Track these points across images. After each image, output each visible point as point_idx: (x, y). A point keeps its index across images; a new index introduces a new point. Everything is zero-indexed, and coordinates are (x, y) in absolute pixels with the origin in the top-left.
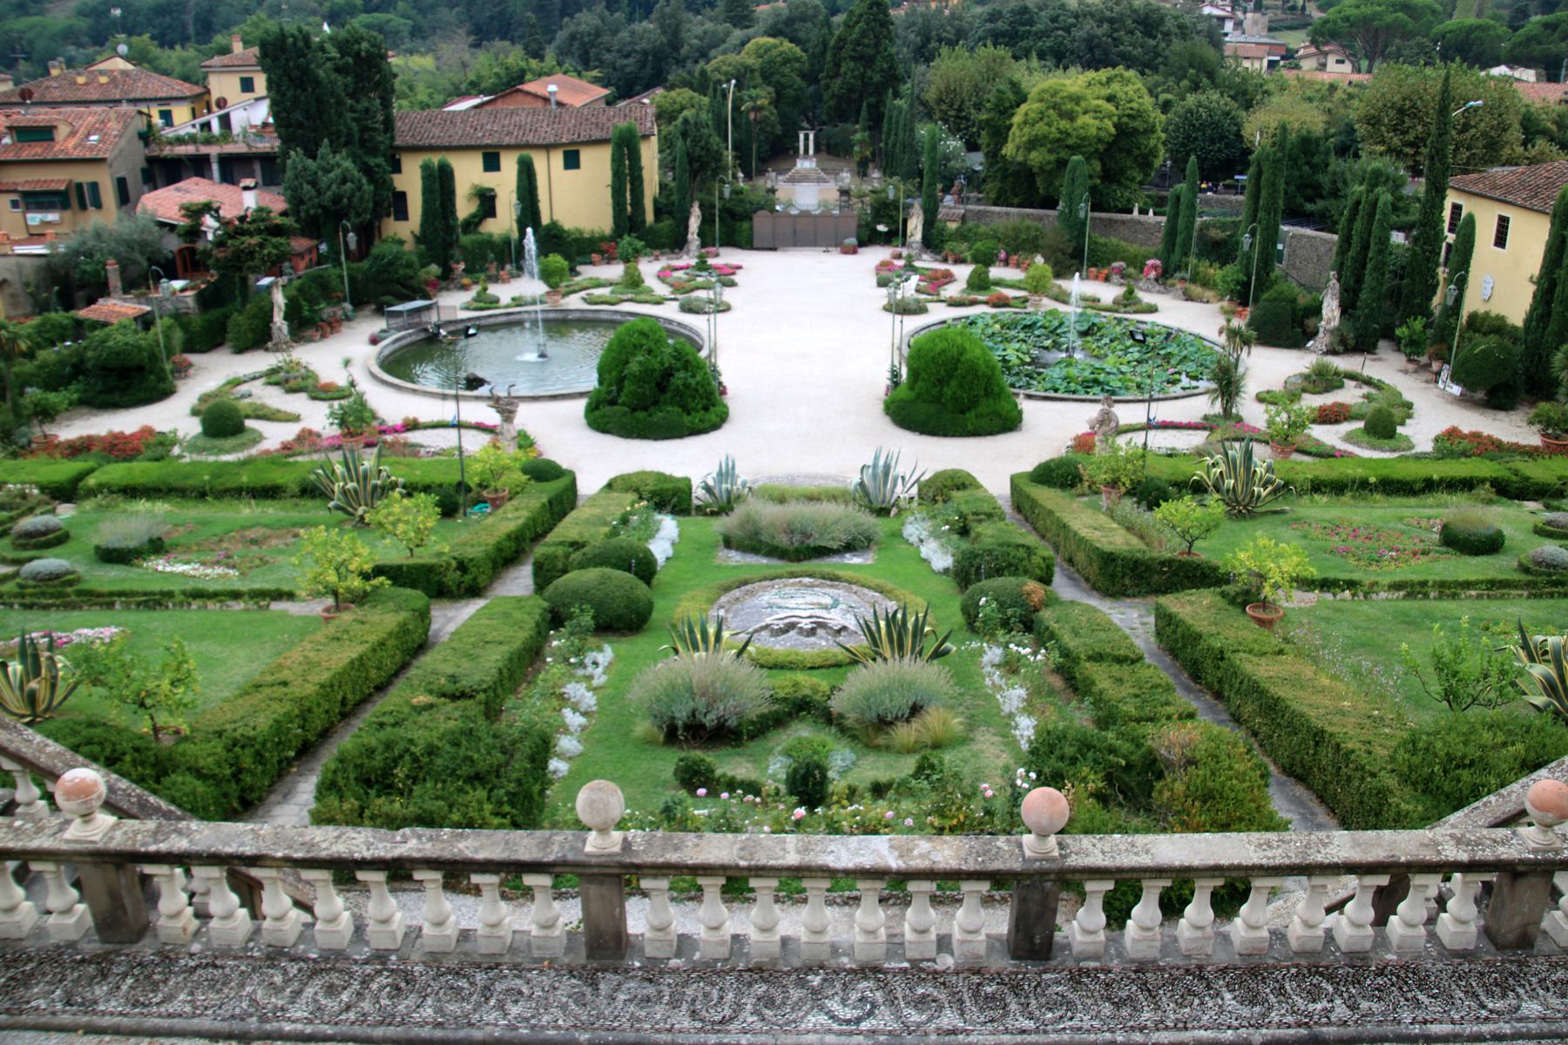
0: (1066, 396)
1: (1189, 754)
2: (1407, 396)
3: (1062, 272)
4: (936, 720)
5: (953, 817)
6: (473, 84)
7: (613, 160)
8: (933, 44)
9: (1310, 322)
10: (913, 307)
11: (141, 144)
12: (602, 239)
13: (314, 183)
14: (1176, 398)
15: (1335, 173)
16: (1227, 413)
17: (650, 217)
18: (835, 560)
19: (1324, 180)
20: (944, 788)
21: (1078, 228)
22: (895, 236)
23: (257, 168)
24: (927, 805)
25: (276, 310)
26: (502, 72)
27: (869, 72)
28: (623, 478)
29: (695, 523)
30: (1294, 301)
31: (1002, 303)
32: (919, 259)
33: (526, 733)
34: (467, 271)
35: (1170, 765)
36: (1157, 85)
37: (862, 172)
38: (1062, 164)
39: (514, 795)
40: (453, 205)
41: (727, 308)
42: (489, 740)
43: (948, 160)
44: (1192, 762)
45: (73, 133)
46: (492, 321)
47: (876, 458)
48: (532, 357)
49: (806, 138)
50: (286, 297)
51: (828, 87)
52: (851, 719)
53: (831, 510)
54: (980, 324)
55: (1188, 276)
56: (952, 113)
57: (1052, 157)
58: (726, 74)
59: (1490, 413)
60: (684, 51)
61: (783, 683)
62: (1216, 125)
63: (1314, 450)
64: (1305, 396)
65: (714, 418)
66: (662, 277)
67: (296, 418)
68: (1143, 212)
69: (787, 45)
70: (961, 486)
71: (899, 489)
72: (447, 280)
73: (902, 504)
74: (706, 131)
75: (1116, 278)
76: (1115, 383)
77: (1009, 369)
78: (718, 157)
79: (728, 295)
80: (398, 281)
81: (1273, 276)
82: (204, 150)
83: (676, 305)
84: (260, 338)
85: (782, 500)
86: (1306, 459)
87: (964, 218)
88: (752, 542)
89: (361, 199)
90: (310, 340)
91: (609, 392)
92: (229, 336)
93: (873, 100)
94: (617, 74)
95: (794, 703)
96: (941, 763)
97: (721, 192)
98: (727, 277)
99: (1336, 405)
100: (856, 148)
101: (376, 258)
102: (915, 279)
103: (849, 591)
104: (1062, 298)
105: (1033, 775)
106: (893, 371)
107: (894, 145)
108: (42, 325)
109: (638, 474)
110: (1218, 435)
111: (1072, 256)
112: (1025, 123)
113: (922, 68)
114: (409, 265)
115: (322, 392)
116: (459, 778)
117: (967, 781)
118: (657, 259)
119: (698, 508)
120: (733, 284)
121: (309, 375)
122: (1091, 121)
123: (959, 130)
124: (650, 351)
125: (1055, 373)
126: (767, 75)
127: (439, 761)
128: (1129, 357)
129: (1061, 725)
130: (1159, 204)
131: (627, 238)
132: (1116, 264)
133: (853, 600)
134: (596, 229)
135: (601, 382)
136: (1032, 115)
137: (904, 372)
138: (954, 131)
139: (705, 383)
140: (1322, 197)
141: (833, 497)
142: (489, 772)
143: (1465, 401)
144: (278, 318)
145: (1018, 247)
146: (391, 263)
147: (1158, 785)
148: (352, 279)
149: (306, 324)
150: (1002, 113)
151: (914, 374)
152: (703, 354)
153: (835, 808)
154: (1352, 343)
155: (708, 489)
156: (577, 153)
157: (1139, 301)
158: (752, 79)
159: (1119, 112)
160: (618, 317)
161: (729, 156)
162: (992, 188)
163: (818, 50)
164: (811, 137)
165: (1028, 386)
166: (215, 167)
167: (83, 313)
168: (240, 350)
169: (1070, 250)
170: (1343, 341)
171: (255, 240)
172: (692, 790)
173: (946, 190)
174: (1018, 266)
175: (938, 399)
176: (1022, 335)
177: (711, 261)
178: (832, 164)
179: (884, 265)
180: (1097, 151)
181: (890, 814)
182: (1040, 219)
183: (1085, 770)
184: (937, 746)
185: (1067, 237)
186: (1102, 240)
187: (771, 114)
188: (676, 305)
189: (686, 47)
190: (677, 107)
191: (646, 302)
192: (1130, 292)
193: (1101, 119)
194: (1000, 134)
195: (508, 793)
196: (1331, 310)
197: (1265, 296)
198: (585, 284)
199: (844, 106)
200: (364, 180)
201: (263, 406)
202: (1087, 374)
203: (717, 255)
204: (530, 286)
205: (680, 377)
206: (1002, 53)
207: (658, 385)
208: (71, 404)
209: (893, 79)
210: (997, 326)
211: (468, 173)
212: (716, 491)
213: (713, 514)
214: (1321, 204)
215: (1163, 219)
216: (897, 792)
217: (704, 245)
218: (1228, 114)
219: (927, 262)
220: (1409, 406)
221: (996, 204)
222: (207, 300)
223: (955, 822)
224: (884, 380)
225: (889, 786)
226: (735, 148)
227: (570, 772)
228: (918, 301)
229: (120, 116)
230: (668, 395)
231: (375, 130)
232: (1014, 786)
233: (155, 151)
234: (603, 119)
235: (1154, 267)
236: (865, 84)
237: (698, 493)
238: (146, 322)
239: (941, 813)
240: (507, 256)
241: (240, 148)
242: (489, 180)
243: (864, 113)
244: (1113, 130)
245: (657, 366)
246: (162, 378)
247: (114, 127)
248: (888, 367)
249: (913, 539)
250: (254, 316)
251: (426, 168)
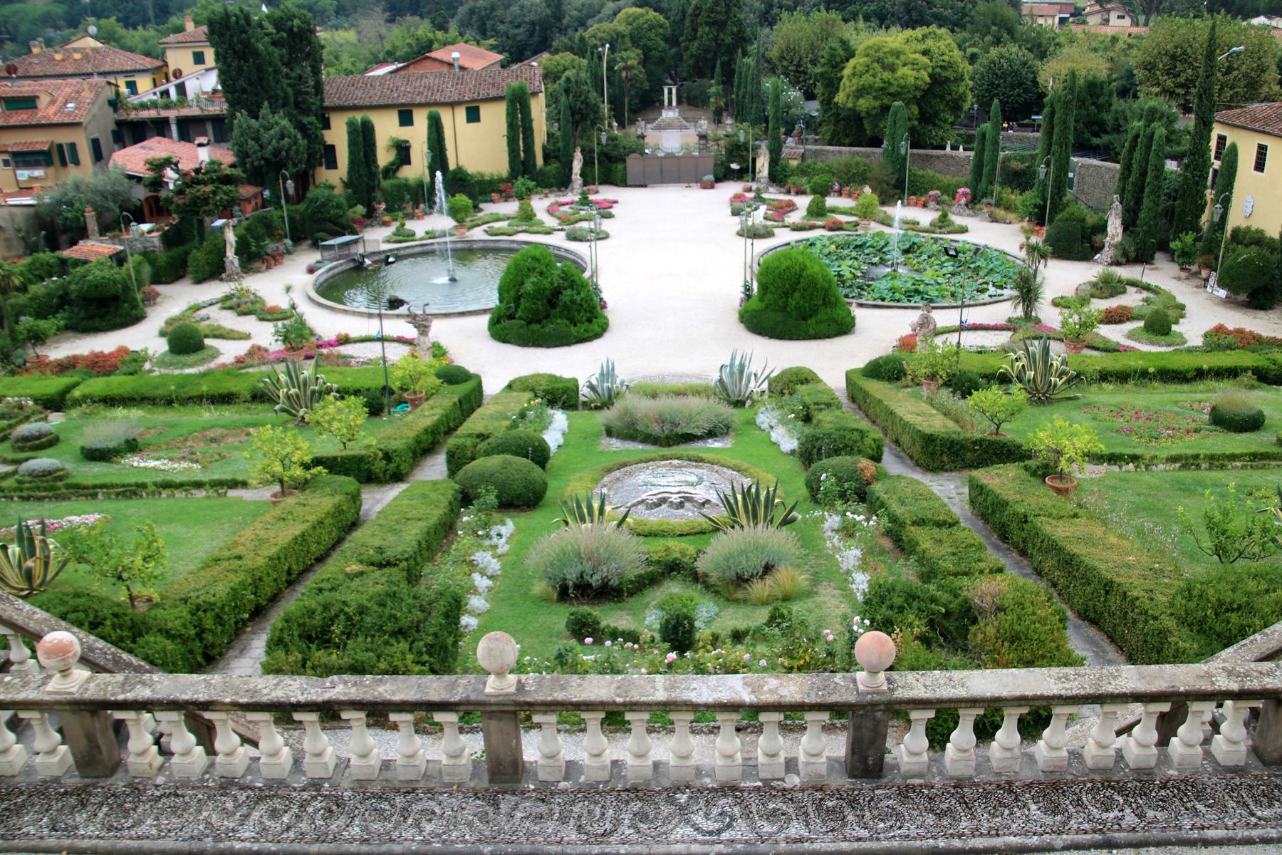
0: (892, 304)
1: (999, 602)
4: (785, 577)
5: (800, 658)
6: (389, 53)
7: (508, 114)
8: (776, 10)
9: (1097, 238)
10: (762, 231)
11: (111, 110)
12: (501, 180)
13: (257, 139)
14: (985, 304)
15: (1117, 112)
16: (1028, 316)
17: (540, 161)
18: (700, 444)
19: (1108, 117)
20: (793, 634)
22: (746, 172)
23: (209, 127)
24: (778, 649)
25: (228, 246)
26: (414, 43)
27: (722, 35)
28: (520, 380)
29: (582, 416)
30: (1083, 220)
31: (837, 227)
32: (767, 192)
33: (441, 594)
34: (388, 210)
35: (982, 611)
36: (965, 41)
37: (717, 119)
38: (885, 109)
39: (432, 646)
40: (375, 155)
41: (606, 236)
42: (411, 601)
43: (790, 108)
44: (1001, 609)
45: (53, 102)
46: (409, 251)
47: (733, 359)
48: (444, 280)
49: (670, 92)
50: (236, 235)
51: (687, 48)
52: (714, 577)
53: (695, 403)
54: (819, 245)
55: (993, 202)
56: (792, 68)
57: (877, 104)
58: (601, 39)
59: (1252, 313)
60: (565, 21)
61: (657, 548)
62: (1016, 73)
63: (1101, 346)
64: (1093, 300)
65: (597, 329)
66: (551, 211)
67: (247, 337)
68: (954, 148)
69: (652, 14)
70: (805, 381)
71: (752, 384)
72: (371, 217)
73: (755, 396)
74: (585, 88)
75: (932, 204)
76: (933, 292)
77: (843, 282)
78: (596, 109)
79: (606, 225)
81: (1065, 199)
82: (164, 114)
83: (563, 234)
84: (215, 271)
85: (654, 395)
87: (803, 157)
88: (629, 431)
89: (297, 152)
90: (258, 271)
91: (509, 308)
92: (190, 269)
93: (725, 59)
94: (510, 42)
95: (666, 565)
96: (789, 612)
97: (599, 139)
98: (605, 211)
99: (1120, 307)
100: (712, 100)
101: (311, 201)
102: (763, 208)
103: (712, 470)
104: (887, 222)
105: (867, 622)
106: (746, 286)
107: (744, 97)
108: (32, 264)
109: (533, 376)
110: (1020, 335)
111: (896, 187)
112: (854, 74)
113: (767, 30)
114: (339, 206)
115: (267, 314)
116: (385, 632)
117: (812, 628)
118: (546, 196)
119: (584, 403)
120: (610, 216)
121: (257, 300)
122: (910, 72)
123: (798, 82)
124: (541, 274)
125: (882, 285)
126: (635, 40)
127: (368, 619)
128: (944, 270)
129: (891, 579)
130: (968, 141)
131: (521, 180)
132: (932, 193)
133: (715, 478)
134: (495, 172)
135: (501, 301)
136: (859, 68)
137: (755, 286)
138: (794, 83)
139: (588, 299)
140: (1106, 132)
141: (697, 392)
142: (410, 628)
143: (1230, 302)
144: (230, 253)
145: (850, 179)
146: (323, 205)
147: (973, 629)
148: (292, 219)
150: (834, 67)
151: (764, 288)
152: (587, 275)
153: (701, 652)
154: (1132, 255)
155: (592, 387)
156: (477, 109)
157: (952, 223)
158: (624, 43)
159: (934, 64)
160: (515, 246)
161: (605, 108)
162: (827, 130)
163: (678, 18)
164: (674, 91)
165: (860, 296)
166: (174, 128)
167: (66, 253)
168: (199, 281)
169: (893, 182)
170: (1125, 254)
171: (210, 188)
172: (581, 641)
173: (788, 133)
174: (850, 196)
175: (784, 309)
176: (854, 254)
177: (592, 197)
178: (692, 113)
179: (737, 197)
180: (915, 97)
181: (747, 656)
182: (868, 156)
183: (912, 617)
184: (786, 598)
185: (891, 170)
186: (920, 173)
187: (640, 72)
188: (563, 234)
189: (568, 18)
190: (561, 68)
191: (538, 233)
192: (945, 216)
193: (918, 70)
194: (833, 85)
195: (426, 645)
196: (1115, 227)
197: (1059, 217)
198: (487, 219)
199: (701, 64)
200: (299, 136)
201: (219, 327)
202: (909, 285)
203: (597, 192)
204: (440, 222)
205: (566, 295)
206: (834, 16)
207: (549, 301)
208: (58, 329)
209: (741, 41)
210: (833, 247)
211: (386, 128)
212: (599, 390)
213: (597, 408)
214: (1105, 139)
215: (972, 154)
216: (753, 638)
217: (585, 184)
218: (1025, 64)
219: (773, 194)
220: (1182, 307)
221: (830, 144)
222: (170, 240)
223: (802, 662)
224: (738, 293)
225: (746, 633)
226: (610, 102)
227: (479, 626)
228: (766, 227)
229: (92, 87)
230: (558, 310)
231: (307, 93)
232: (851, 631)
233: (123, 116)
234: (498, 80)
235: (965, 194)
236: (719, 46)
237: (584, 390)
238: (119, 259)
239: (790, 654)
240: (421, 197)
241: (195, 111)
242: (404, 133)
243: (718, 70)
244: (928, 80)
245: (547, 286)
246: (135, 307)
247: (87, 95)
248: (742, 282)
249: (765, 426)
250: (210, 252)
251: (351, 125)
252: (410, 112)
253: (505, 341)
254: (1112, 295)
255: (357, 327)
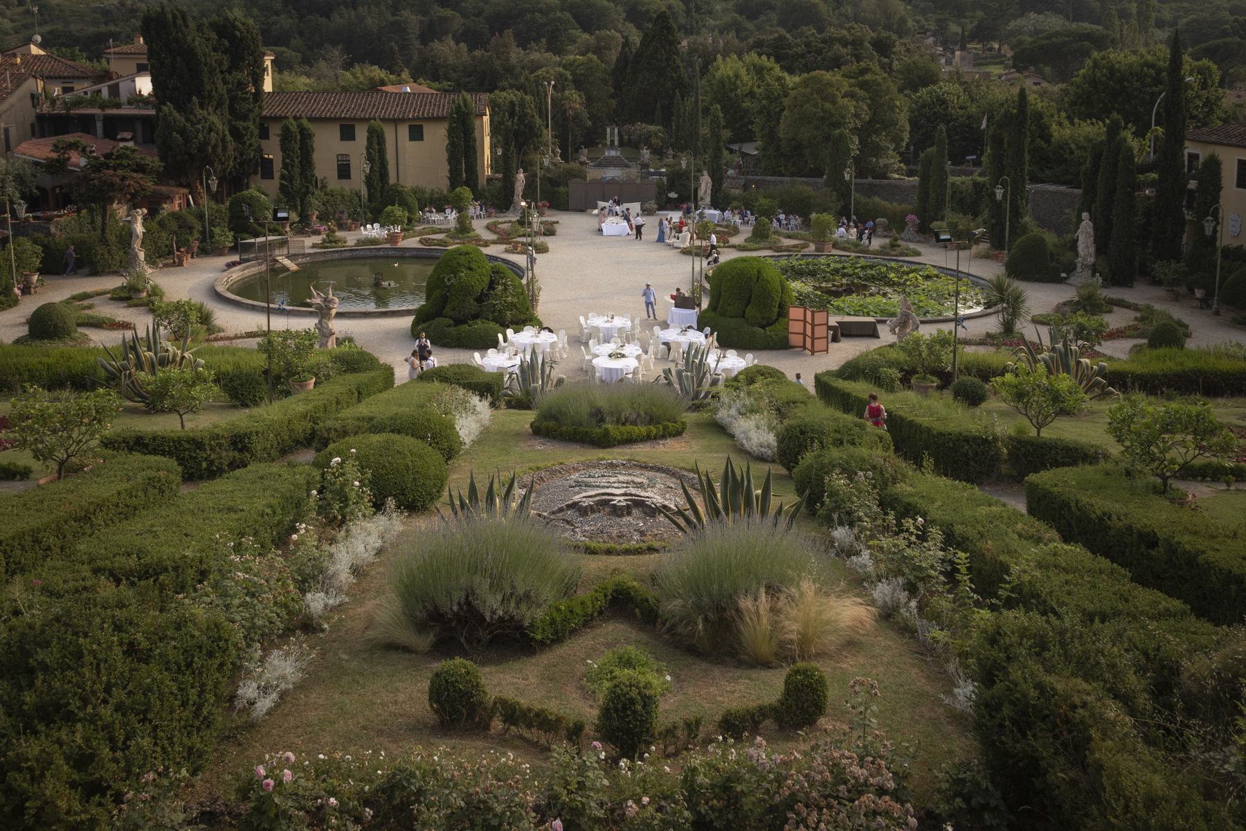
11: (30, 103)
23: (139, 127)
49: (612, 133)
97: (542, 164)
161: (548, 134)
166: (99, 125)
252: (353, 127)
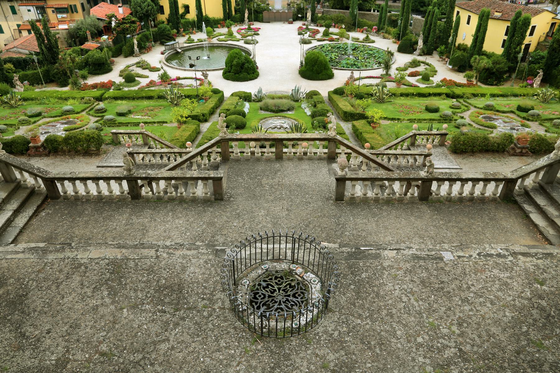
0: (346, 69)
2: (437, 69)
3: (349, 29)
9: (415, 46)
10: (308, 42)
16: (387, 74)
21: (354, 17)
22: (303, 18)
31: (332, 40)
32: (310, 25)
46: (193, 47)
48: (206, 58)
53: (284, 101)
54: (325, 47)
59: (458, 73)
64: (409, 68)
65: (256, 76)
66: (238, 32)
67: (147, 77)
68: (374, 11)
70: (317, 95)
71: (301, 94)
73: (302, 99)
77: (332, 61)
80: (166, 35)
81: (407, 32)
83: (243, 41)
86: (405, 87)
87: (323, 13)
91: (229, 69)
92: (123, 53)
97: (253, 6)
98: (256, 32)
99: (417, 71)
103: (288, 120)
110: (384, 80)
111: (353, 25)
119: (253, 100)
120: (258, 34)
121: (148, 64)
124: (239, 58)
125: (344, 62)
131: (228, 21)
133: (289, 122)
135: (226, 67)
139: (253, 67)
141: (286, 97)
149: (144, 48)
152: (251, 57)
154: (426, 52)
155: (255, 95)
157: (370, 39)
160: (228, 45)
167: (82, 47)
169: (352, 23)
170: (423, 52)
173: (318, 3)
174: (338, 28)
175: (312, 70)
176: (336, 50)
177: (252, 27)
179: (300, 28)
182: (344, 13)
185: (352, 19)
186: (361, 20)
191: (235, 41)
192: (368, 37)
196: (420, 43)
198: (217, 35)
203: (253, 25)
210: (330, 48)
213: (257, 101)
217: (249, 21)
219: (312, 27)
220: (436, 71)
222: (116, 41)
224: (299, 64)
235: (375, 29)
238: (101, 49)
248: (300, 61)
253: (228, 79)
254: (415, 67)
255: (182, 74)
